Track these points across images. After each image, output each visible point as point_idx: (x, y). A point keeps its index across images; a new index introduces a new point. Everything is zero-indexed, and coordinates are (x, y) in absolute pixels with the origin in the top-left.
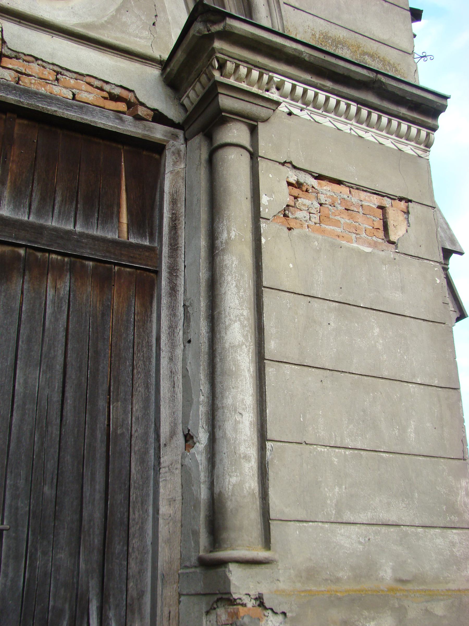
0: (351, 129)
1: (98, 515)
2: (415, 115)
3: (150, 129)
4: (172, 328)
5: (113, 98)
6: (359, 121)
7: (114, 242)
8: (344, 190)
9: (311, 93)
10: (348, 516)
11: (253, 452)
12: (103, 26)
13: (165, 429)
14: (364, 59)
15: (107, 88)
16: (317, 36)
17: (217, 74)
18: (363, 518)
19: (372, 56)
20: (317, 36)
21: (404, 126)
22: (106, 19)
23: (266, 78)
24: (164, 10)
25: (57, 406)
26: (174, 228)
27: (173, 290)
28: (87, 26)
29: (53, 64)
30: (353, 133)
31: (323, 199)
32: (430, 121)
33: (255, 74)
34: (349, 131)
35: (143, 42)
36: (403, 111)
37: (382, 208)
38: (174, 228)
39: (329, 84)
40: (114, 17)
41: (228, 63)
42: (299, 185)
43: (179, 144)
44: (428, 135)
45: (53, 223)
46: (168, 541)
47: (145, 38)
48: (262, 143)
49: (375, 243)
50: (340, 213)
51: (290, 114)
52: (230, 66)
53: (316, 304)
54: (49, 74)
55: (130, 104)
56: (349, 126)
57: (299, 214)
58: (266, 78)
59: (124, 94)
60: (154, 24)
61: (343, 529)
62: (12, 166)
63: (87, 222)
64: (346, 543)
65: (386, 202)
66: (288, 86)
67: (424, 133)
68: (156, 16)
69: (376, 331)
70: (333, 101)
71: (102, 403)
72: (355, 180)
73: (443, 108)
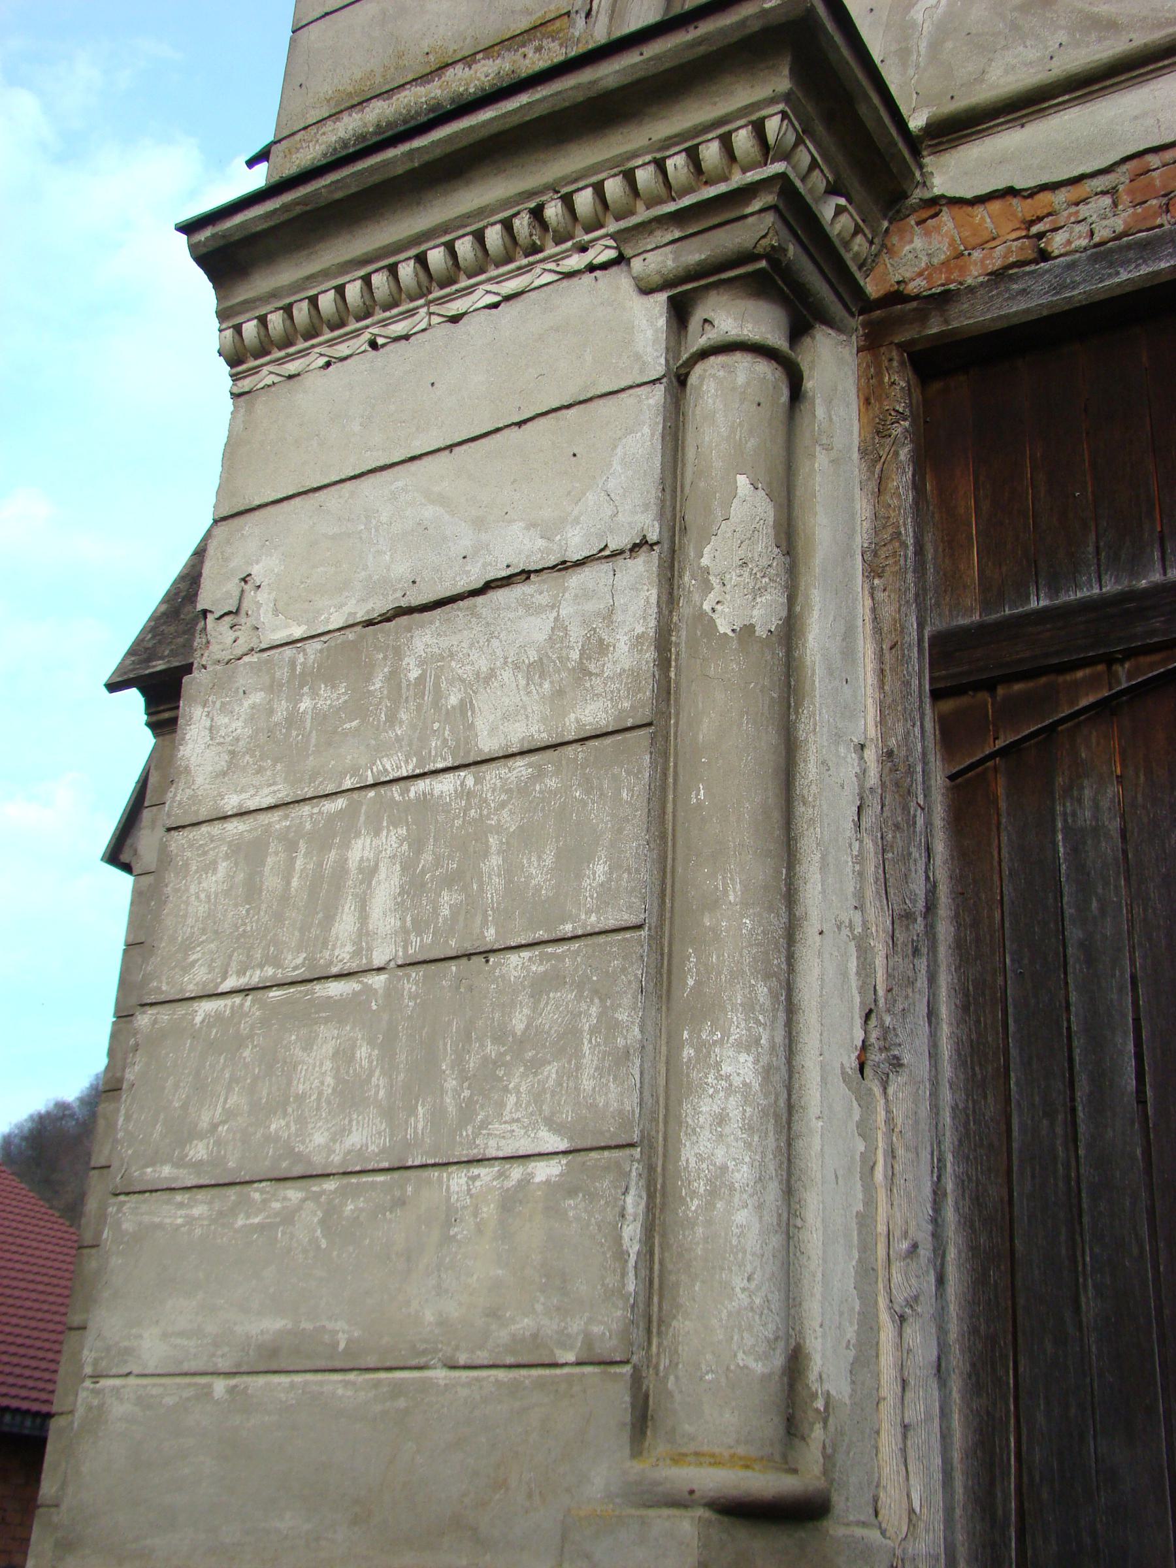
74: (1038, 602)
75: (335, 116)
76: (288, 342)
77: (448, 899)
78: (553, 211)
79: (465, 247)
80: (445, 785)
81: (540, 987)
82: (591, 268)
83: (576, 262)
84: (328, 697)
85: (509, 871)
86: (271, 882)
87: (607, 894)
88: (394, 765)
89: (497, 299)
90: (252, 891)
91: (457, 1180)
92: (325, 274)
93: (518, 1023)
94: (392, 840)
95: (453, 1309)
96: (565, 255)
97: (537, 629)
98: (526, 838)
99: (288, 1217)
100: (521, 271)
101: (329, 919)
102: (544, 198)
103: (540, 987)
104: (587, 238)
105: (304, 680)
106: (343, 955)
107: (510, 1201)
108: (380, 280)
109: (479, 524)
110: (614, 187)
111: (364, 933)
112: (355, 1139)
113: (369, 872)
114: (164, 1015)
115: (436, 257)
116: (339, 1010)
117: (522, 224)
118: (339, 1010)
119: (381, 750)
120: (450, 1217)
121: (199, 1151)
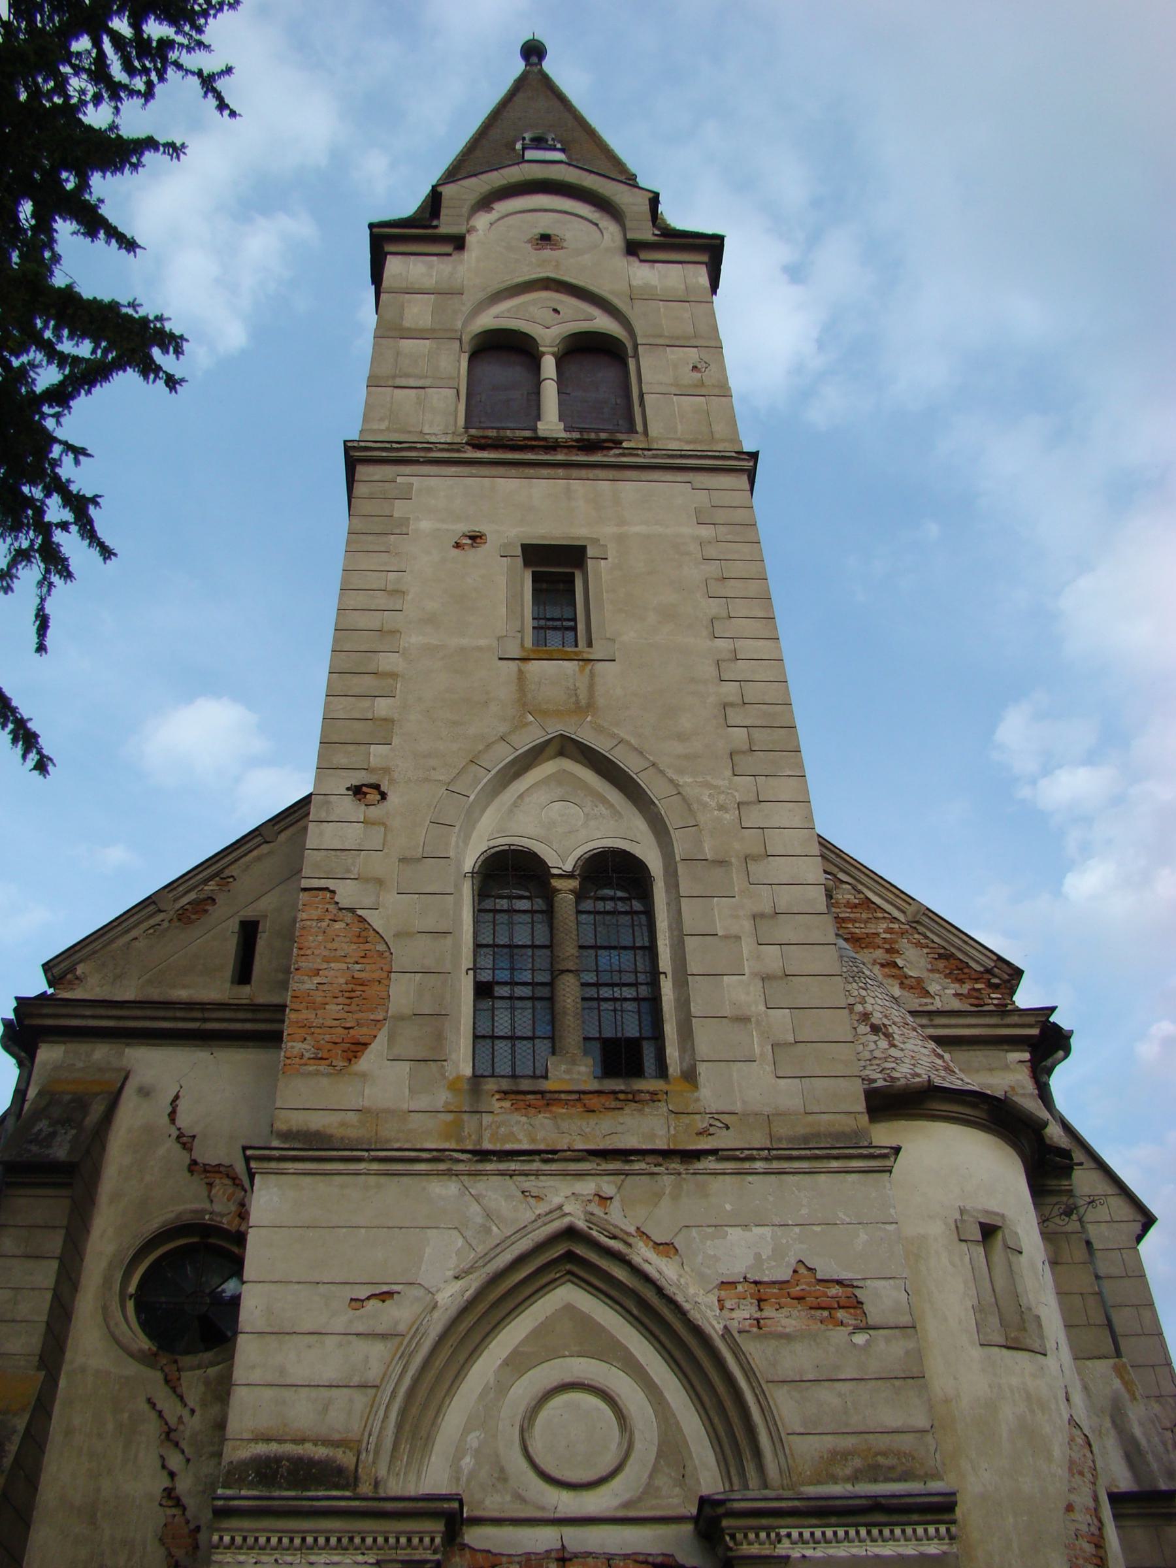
0: (866, 1550)
2: (929, 1517)
6: (873, 1540)
9: (818, 1533)
12: (640, 1499)
14: (876, 1461)
15: (651, 1559)
16: (825, 1457)
17: (731, 1544)
19: (884, 1454)
20: (825, 1457)
21: (920, 1530)
22: (641, 1490)
23: (773, 1535)
24: (691, 1458)
28: (626, 1505)
29: (604, 1553)
30: (869, 1553)
32: (946, 1517)
33: (763, 1535)
34: (864, 1553)
35: (675, 1501)
36: (915, 1517)
39: (833, 1520)
40: (648, 1485)
41: (737, 1535)
44: (948, 1530)
47: (677, 1496)
51: (804, 1556)
52: (739, 1536)
56: (864, 1548)
58: (773, 1535)
60: (683, 1476)
67: (943, 1529)
68: (684, 1468)
70: (841, 1532)
73: (955, 1503)
75: (255, 1440)
76: (240, 1548)
78: (357, 1540)
79: (321, 1540)
82: (366, 1563)
83: (360, 1558)
89: (328, 1561)
92: (264, 1530)
96: (357, 1555)
100: (340, 1554)
102: (354, 1534)
104: (366, 1552)
108: (285, 1541)
110: (380, 1540)
115: (310, 1540)
117: (345, 1541)
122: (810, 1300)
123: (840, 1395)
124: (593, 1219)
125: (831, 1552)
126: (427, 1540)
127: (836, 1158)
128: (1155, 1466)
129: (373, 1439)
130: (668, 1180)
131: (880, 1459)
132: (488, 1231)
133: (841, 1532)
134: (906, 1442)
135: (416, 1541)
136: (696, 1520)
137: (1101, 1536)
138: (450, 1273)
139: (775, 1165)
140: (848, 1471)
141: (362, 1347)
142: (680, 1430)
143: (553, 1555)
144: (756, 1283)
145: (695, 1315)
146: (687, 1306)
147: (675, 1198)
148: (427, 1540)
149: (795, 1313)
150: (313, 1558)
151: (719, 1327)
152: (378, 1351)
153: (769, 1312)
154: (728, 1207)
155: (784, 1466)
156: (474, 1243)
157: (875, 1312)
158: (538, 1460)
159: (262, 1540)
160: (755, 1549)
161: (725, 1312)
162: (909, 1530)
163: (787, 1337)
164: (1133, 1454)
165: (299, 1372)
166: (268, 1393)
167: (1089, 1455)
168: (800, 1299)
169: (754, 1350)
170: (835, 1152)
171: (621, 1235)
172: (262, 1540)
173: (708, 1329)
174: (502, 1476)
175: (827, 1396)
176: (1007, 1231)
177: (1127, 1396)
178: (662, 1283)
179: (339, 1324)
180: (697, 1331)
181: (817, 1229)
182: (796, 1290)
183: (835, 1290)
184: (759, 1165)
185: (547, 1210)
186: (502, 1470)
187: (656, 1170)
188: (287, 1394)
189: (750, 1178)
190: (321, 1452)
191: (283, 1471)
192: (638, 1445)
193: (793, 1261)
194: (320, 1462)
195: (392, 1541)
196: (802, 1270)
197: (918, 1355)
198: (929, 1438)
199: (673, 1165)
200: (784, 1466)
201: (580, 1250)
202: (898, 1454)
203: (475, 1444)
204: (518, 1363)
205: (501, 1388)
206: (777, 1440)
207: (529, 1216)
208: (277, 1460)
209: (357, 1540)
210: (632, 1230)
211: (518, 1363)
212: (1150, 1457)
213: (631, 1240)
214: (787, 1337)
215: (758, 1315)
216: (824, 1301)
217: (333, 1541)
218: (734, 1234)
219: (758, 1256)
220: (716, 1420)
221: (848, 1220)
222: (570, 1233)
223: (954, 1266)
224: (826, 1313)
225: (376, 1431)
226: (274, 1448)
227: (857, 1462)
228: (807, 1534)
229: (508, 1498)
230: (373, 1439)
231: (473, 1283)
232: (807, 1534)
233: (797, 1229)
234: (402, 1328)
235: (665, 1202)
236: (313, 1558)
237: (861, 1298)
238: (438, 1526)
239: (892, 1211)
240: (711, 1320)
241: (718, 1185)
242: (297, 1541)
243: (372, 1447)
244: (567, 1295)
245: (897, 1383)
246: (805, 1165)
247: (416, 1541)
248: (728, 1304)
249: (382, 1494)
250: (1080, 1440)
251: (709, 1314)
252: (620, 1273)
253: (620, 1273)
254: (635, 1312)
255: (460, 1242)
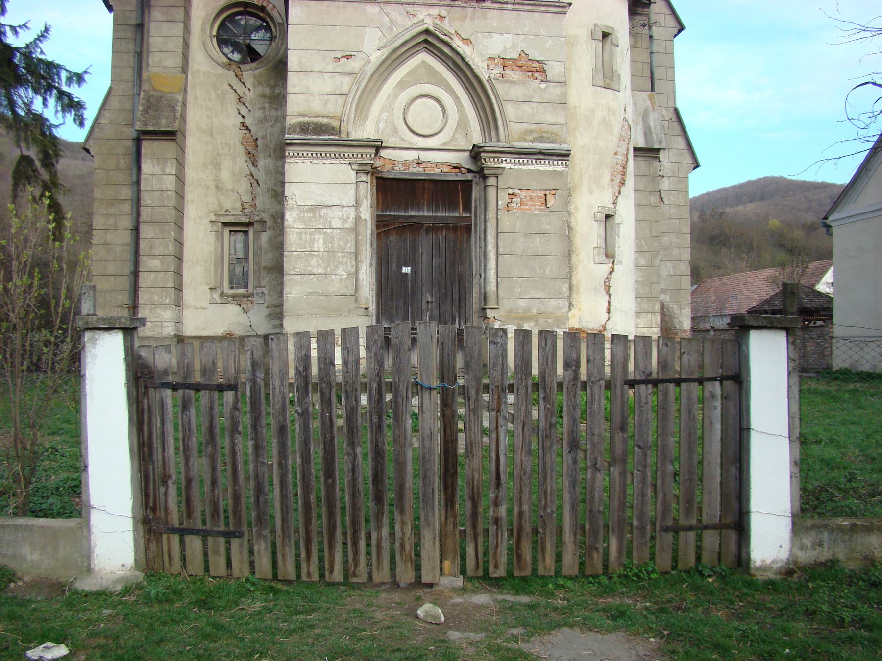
1: (457, 296)
2: (560, 158)
3: (467, 177)
4: (476, 243)
5: (455, 168)
7: (458, 217)
8: (530, 193)
9: (517, 160)
10: (523, 296)
11: (495, 281)
13: (474, 273)
18: (528, 297)
19: (546, 132)
21: (555, 162)
25: (444, 270)
26: (476, 210)
27: (476, 231)
28: (444, 144)
31: (522, 197)
33: (496, 160)
36: (554, 158)
37: (545, 195)
38: (476, 210)
39: (523, 156)
42: (513, 194)
43: (477, 179)
45: (439, 214)
46: (476, 303)
48: (499, 183)
49: (541, 209)
50: (528, 201)
52: (487, 160)
53: (516, 234)
54: (433, 165)
55: (459, 168)
57: (513, 205)
59: (458, 165)
61: (521, 300)
62: (426, 196)
63: (450, 212)
64: (522, 303)
65: (547, 192)
66: (508, 160)
67: (564, 162)
69: (538, 240)
70: (526, 161)
71: (457, 266)
72: (535, 188)
74: (388, 213)
75: (299, 116)
77: (330, 245)
78: (342, 155)
79: (328, 155)
80: (329, 231)
81: (343, 257)
83: (343, 162)
84: (309, 215)
85: (338, 243)
86: (304, 238)
87: (350, 248)
88: (321, 226)
90: (301, 239)
91: (334, 277)
93: (340, 260)
94: (321, 236)
95: (334, 290)
97: (340, 214)
98: (340, 239)
99: (312, 279)
101: (313, 245)
103: (343, 257)
105: (305, 211)
106: (316, 249)
107: (340, 279)
108: (314, 155)
109: (330, 196)
110: (351, 155)
111: (318, 247)
112: (320, 271)
113: (318, 240)
114: (289, 253)
115: (323, 155)
116: (316, 256)
117: (337, 155)
118: (316, 256)
119: (319, 224)
120: (333, 280)
121: (298, 270)
122: (525, 68)
123: (532, 108)
124: (437, 26)
125: (521, 167)
126: (369, 156)
127: (544, 6)
128: (655, 138)
129: (346, 117)
130: (470, 10)
131: (544, 134)
132: (392, 29)
133: (526, 161)
134: (555, 129)
135: (364, 156)
136: (471, 151)
137: (626, 164)
138: (376, 48)
139: (517, 7)
140: (531, 138)
141: (339, 79)
142: (467, 116)
143: (415, 161)
144: (503, 59)
145: (477, 71)
146: (474, 67)
147: (472, 18)
148: (369, 156)
149: (518, 73)
150: (325, 161)
151: (486, 77)
152: (347, 80)
153: (507, 71)
154: (495, 24)
155: (507, 134)
156: (385, 34)
157: (550, 75)
158: (410, 125)
159: (305, 154)
160: (492, 165)
161: (489, 70)
162: (551, 162)
163: (514, 83)
164: (647, 133)
165: (314, 88)
166: (303, 97)
167: (629, 132)
168: (521, 67)
169: (501, 88)
170: (543, 3)
171: (447, 33)
172: (305, 154)
173: (482, 77)
174: (396, 131)
175: (527, 108)
176: (613, 36)
177: (651, 109)
178: (464, 56)
179: (330, 68)
180: (477, 77)
181: (531, 37)
182: (519, 63)
183: (535, 64)
184: (510, 6)
185: (417, 21)
186: (396, 128)
187: (465, 5)
188: (310, 97)
189: (505, 12)
190: (325, 121)
191: (311, 128)
192: (450, 121)
193: (519, 50)
194: (325, 125)
195: (355, 156)
196: (523, 55)
197: (565, 94)
198: (564, 128)
199: (472, 4)
200: (507, 134)
201: (430, 39)
202: (552, 133)
203: (385, 118)
204: (402, 85)
205: (396, 96)
206: (505, 124)
207: (409, 23)
208: (308, 124)
209: (342, 155)
210: (453, 32)
211: (402, 85)
212: (654, 135)
213: (452, 37)
214: (514, 83)
215: (503, 73)
216: (530, 69)
217: (333, 155)
218: (496, 37)
219: (505, 47)
220: (481, 113)
221: (544, 34)
222: (427, 32)
223: (588, 50)
224: (530, 74)
225: (347, 113)
226: (306, 119)
227: (535, 135)
228: (513, 160)
229: (398, 139)
230: (346, 117)
231: (386, 52)
232: (513, 160)
233: (523, 36)
234: (356, 71)
235: (468, 20)
236: (325, 161)
237: (546, 69)
238: (373, 151)
239: (564, 32)
240: (483, 74)
241: (491, 13)
242: (319, 155)
243: (346, 119)
244: (424, 57)
245: (555, 105)
246: (530, 8)
247: (364, 156)
248: (491, 67)
249: (350, 138)
250: (626, 127)
251: (483, 71)
252: (446, 50)
253: (446, 50)
254: (452, 66)
255: (380, 34)
